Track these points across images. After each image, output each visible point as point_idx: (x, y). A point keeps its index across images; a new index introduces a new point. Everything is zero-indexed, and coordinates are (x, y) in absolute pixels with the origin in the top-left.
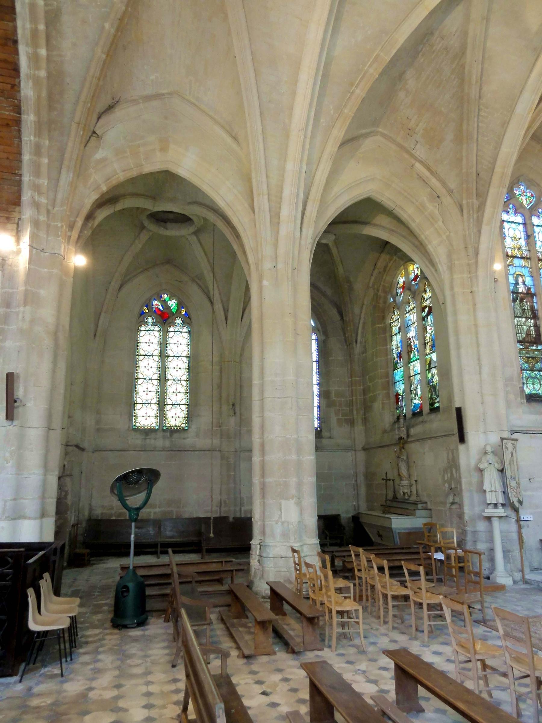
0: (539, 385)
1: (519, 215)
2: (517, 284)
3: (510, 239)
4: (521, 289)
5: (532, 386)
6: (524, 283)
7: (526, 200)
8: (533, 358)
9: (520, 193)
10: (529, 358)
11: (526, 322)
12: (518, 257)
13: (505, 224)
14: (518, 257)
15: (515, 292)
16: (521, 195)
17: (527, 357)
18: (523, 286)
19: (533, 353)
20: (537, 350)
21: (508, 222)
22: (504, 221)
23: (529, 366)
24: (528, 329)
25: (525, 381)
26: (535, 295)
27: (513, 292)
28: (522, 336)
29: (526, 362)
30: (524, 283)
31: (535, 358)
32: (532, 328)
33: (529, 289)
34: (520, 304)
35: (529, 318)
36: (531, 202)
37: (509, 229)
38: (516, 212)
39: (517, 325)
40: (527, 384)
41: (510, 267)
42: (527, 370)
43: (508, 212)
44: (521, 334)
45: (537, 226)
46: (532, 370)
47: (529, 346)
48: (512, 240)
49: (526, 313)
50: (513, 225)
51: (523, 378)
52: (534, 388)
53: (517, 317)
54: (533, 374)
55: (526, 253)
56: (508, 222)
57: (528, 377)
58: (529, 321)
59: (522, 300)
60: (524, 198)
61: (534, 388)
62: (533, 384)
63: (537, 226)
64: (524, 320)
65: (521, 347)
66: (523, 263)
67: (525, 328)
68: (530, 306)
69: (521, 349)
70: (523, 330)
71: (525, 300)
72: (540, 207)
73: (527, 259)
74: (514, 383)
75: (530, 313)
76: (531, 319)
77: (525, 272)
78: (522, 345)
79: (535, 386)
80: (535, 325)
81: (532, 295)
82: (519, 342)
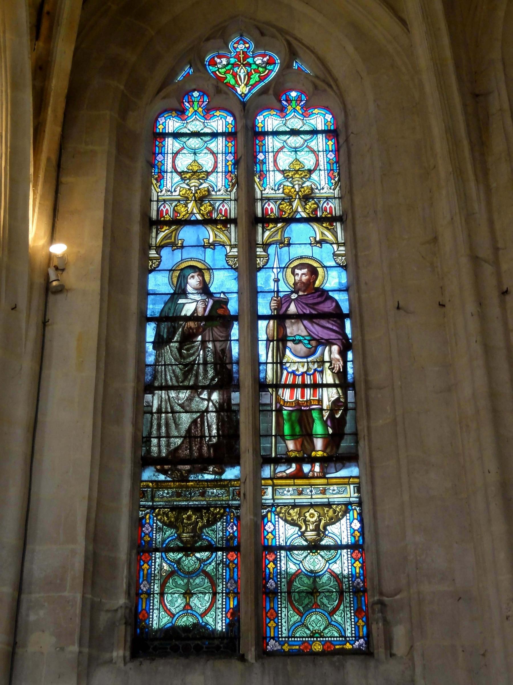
0: (208, 597)
1: (217, 113)
2: (181, 292)
3: (177, 178)
4: (189, 307)
5: (180, 602)
6: (204, 289)
7: (249, 75)
8: (197, 509)
9: (232, 60)
10: (186, 509)
11: (190, 399)
12: (196, 223)
13: (170, 141)
14: (196, 223)
15: (169, 320)
16: (234, 65)
17: (173, 508)
18: (198, 297)
19: (203, 494)
20: (217, 483)
21: (176, 135)
22: (164, 135)
23: (179, 538)
24: (194, 422)
25: (157, 588)
26: (236, 318)
27: (158, 320)
28: (168, 445)
29: (170, 525)
30: (204, 289)
31: (207, 508)
32: (212, 417)
33: (221, 303)
34: (179, 350)
35: (204, 388)
36: (262, 79)
37: (178, 153)
38: (208, 112)
39: (159, 411)
40: (162, 594)
41: (165, 252)
42: (168, 550)
43: (181, 113)
44: (168, 436)
45: (275, 133)
46: (188, 549)
47: (189, 472)
48: (182, 179)
49: (197, 376)
50: (194, 142)
51: (149, 578)
52: (187, 607)
53: (161, 388)
54: (190, 562)
55: (230, 209)
56: (176, 135)
57: (171, 574)
58: (205, 395)
59: (188, 338)
60: (242, 72)
61: (187, 607)
62: (188, 594)
63: (275, 133)
64: (184, 395)
65: (162, 477)
66: (209, 234)
67: (186, 419)
68: (215, 352)
69: (159, 485)
70: (177, 425)
71: (200, 338)
72: (289, 85)
73: (226, 222)
74: (66, 594)
75: (211, 373)
76: (211, 389)
77: (214, 258)
78: (165, 472)
79: (195, 601)
80: (225, 409)
81: (227, 321)
82: (147, 461)
